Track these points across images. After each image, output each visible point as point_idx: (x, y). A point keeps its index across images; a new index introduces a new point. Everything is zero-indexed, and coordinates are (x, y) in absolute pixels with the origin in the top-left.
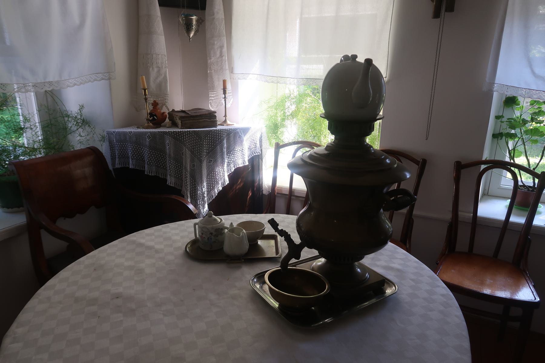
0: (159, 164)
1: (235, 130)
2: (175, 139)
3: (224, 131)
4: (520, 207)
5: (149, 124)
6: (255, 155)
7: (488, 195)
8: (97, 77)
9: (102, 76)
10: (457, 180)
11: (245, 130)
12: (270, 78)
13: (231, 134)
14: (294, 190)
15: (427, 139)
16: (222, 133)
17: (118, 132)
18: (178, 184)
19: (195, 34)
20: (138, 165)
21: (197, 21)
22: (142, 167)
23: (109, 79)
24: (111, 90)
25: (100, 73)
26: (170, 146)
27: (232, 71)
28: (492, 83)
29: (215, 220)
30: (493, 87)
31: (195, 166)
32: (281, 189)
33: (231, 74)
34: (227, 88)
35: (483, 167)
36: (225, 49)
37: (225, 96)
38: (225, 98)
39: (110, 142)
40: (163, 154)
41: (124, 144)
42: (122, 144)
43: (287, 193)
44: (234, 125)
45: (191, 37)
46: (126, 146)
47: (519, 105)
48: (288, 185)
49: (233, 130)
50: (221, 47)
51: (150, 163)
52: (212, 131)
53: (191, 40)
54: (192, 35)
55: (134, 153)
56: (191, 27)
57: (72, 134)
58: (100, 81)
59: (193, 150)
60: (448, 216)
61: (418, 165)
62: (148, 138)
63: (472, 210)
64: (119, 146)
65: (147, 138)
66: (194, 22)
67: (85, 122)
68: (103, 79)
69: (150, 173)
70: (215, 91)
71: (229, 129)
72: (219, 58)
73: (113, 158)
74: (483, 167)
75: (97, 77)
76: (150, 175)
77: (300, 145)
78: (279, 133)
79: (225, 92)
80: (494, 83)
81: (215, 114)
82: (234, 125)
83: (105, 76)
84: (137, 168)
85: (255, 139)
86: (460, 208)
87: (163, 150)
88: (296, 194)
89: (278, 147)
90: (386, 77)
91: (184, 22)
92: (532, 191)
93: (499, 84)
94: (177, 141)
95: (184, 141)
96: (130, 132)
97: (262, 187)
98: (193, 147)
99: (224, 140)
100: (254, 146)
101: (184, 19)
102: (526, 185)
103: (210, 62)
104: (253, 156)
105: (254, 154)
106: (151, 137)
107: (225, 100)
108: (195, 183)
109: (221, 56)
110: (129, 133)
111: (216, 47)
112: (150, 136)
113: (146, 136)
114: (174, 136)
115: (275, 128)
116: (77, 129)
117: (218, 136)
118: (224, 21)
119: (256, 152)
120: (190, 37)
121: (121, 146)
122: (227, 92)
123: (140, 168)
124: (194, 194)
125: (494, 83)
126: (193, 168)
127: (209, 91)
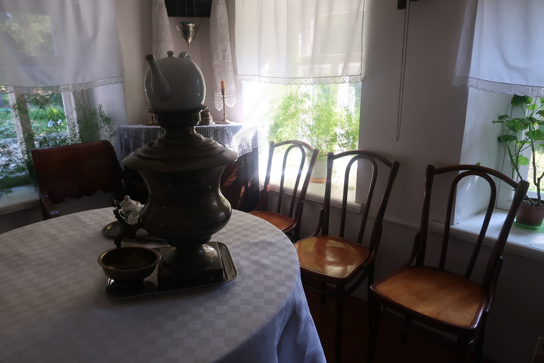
1: (222, 128)
3: (211, 129)
4: (522, 225)
5: (153, 122)
6: (247, 152)
7: (497, 208)
8: (112, 81)
9: (116, 80)
10: (429, 186)
11: (235, 130)
12: (275, 79)
13: (219, 131)
14: (285, 189)
15: (397, 140)
16: (209, 130)
17: (124, 128)
19: (193, 40)
21: (194, 28)
23: (122, 82)
24: (124, 92)
25: (115, 77)
27: (235, 72)
28: (465, 77)
29: (131, 203)
30: (467, 81)
32: (274, 187)
33: (236, 76)
34: (225, 89)
35: (461, 172)
36: (229, 52)
37: (224, 96)
38: (223, 98)
39: (121, 136)
43: (278, 191)
44: (230, 123)
45: (189, 42)
47: (529, 103)
48: (279, 184)
49: (221, 128)
50: (224, 51)
52: (199, 128)
53: (189, 45)
54: (190, 41)
56: (187, 34)
57: (101, 129)
58: (115, 84)
60: (417, 225)
61: (390, 167)
63: (444, 220)
66: (191, 29)
67: (107, 120)
68: (117, 82)
70: (218, 92)
71: (217, 127)
72: (221, 61)
74: (461, 172)
75: (112, 81)
77: (292, 144)
78: (278, 132)
79: (223, 93)
80: (468, 77)
81: (208, 113)
82: (230, 123)
83: (119, 80)
85: (246, 137)
86: (431, 217)
88: (287, 193)
89: (273, 146)
90: (361, 74)
91: (182, 29)
92: (537, 205)
93: (473, 78)
96: (132, 128)
97: (259, 184)
99: (211, 137)
100: (245, 144)
101: (182, 26)
102: (529, 197)
103: (214, 65)
104: (245, 153)
105: (246, 151)
106: (146, 132)
107: (224, 100)
109: (224, 58)
110: (130, 129)
111: (219, 51)
115: (275, 128)
116: (105, 126)
117: (205, 133)
118: (227, 26)
119: (247, 150)
120: (188, 42)
122: (225, 93)
125: (468, 77)
127: (215, 92)
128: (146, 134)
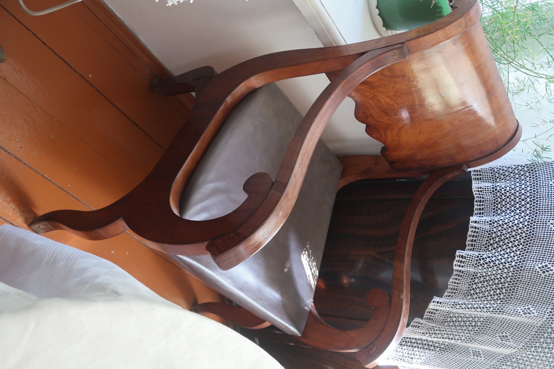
0: (481, 282)
2: (540, 327)
18: (435, 314)
20: (477, 232)
22: (472, 241)
26: (525, 316)
31: (475, 357)
40: (503, 293)
41: (528, 206)
42: (528, 200)
46: (523, 209)
51: (481, 265)
55: (505, 229)
59: (514, 360)
62: (543, 267)
64: (523, 192)
65: (544, 264)
69: (459, 263)
73: (495, 175)
76: (455, 263)
84: (470, 229)
87: (512, 295)
94: (536, 332)
95: (536, 347)
98: (521, 361)
108: (438, 349)
112: (548, 271)
113: (547, 263)
114: (548, 328)
121: (523, 197)
123: (470, 236)
124: (414, 343)
126: (472, 352)
128: (541, 272)
